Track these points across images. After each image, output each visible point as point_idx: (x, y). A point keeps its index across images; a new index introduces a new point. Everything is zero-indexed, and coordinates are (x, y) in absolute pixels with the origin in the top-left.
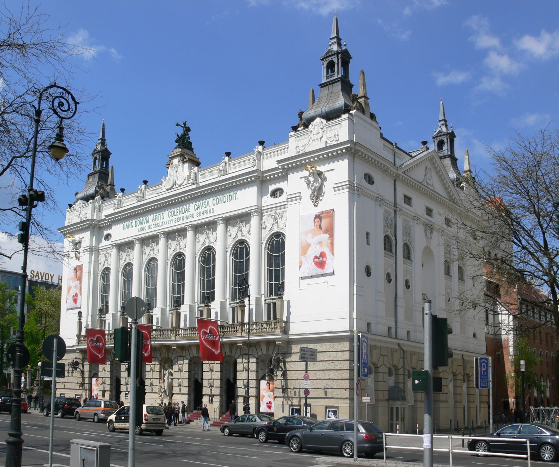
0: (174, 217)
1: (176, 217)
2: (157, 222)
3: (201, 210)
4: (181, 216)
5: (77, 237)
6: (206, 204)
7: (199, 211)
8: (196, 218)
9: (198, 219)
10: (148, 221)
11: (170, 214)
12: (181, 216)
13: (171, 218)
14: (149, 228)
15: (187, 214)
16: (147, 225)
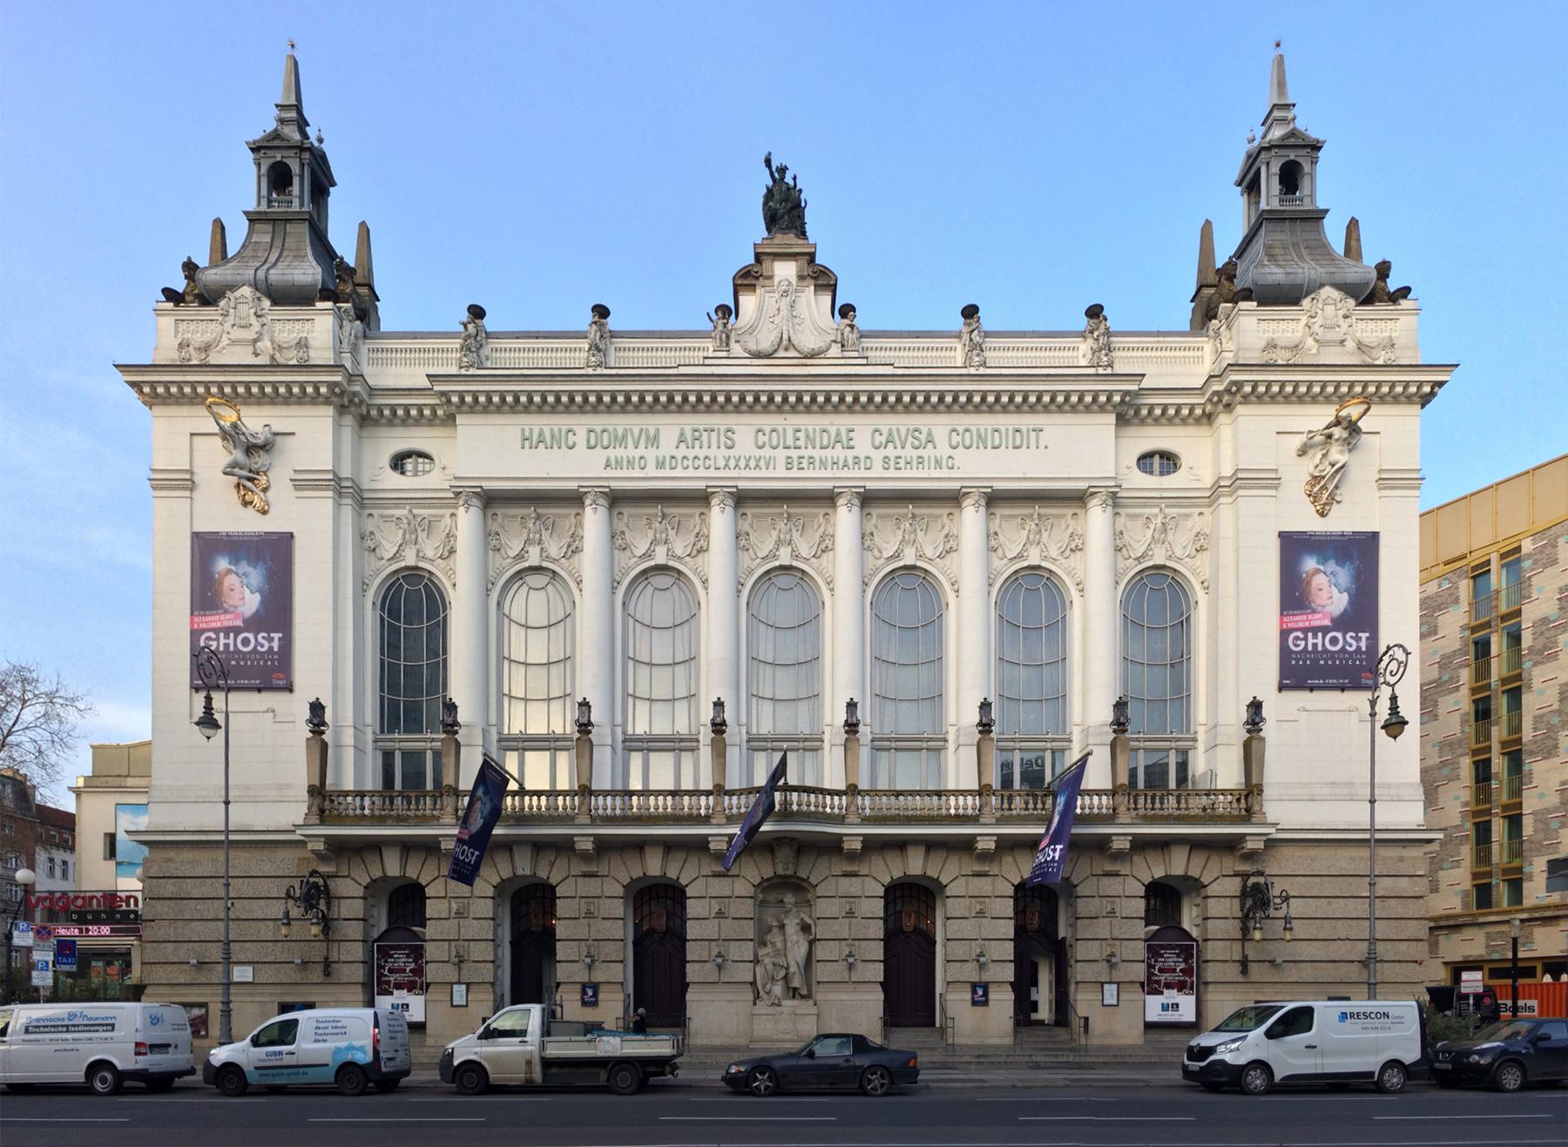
0: (781, 454)
1: (794, 453)
2: (691, 453)
3: (899, 452)
4: (817, 453)
5: (255, 421)
6: (923, 437)
7: (890, 451)
8: (877, 471)
9: (880, 477)
10: (654, 441)
11: (762, 439)
12: (817, 453)
13: (767, 452)
14: (660, 465)
15: (839, 453)
16: (651, 455)
